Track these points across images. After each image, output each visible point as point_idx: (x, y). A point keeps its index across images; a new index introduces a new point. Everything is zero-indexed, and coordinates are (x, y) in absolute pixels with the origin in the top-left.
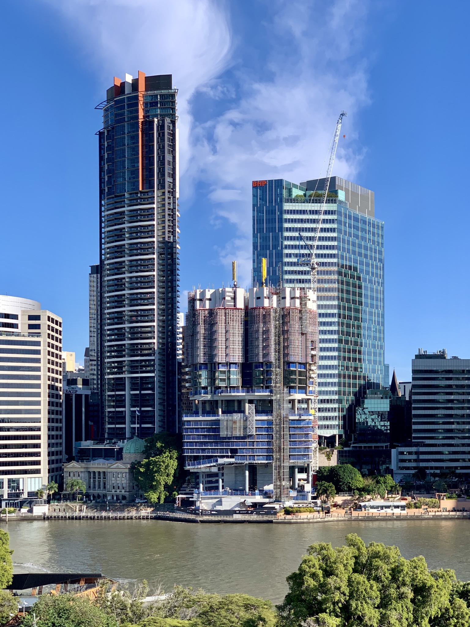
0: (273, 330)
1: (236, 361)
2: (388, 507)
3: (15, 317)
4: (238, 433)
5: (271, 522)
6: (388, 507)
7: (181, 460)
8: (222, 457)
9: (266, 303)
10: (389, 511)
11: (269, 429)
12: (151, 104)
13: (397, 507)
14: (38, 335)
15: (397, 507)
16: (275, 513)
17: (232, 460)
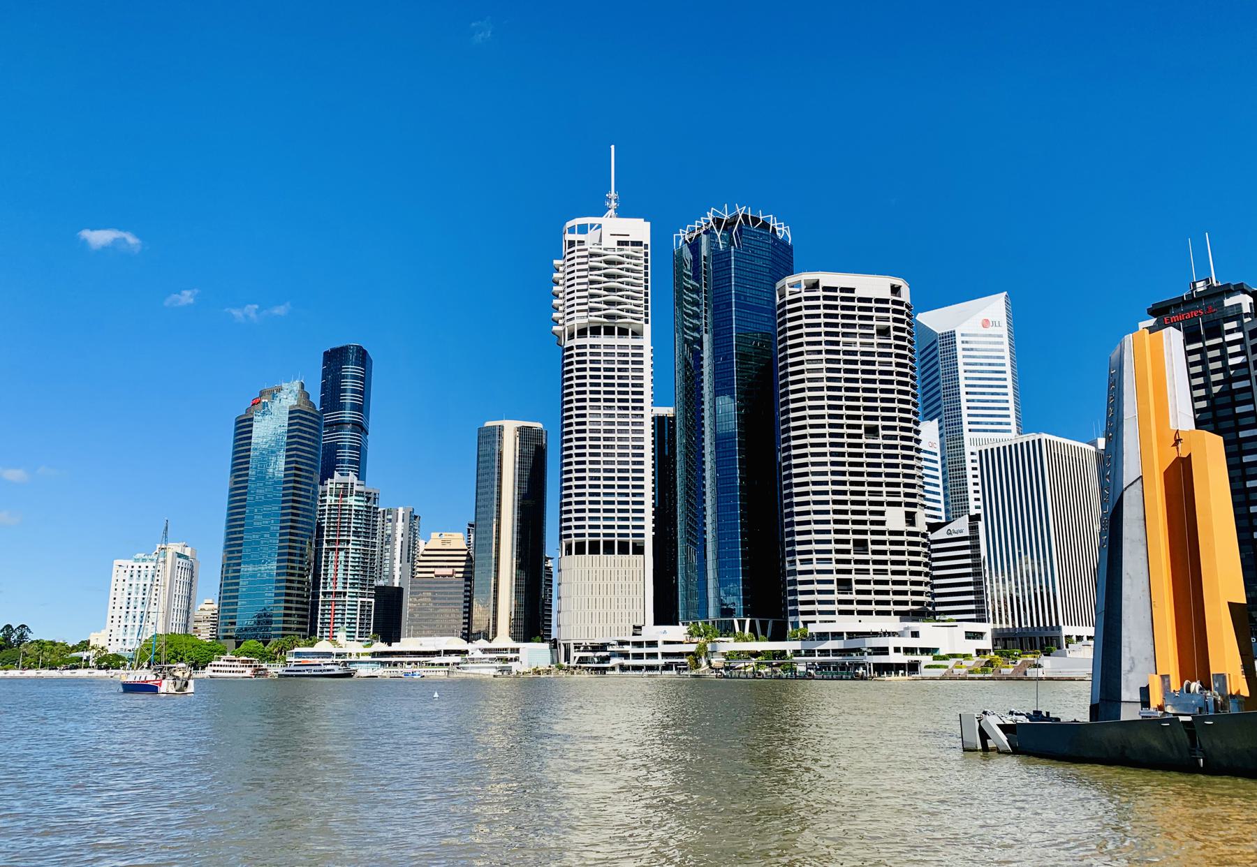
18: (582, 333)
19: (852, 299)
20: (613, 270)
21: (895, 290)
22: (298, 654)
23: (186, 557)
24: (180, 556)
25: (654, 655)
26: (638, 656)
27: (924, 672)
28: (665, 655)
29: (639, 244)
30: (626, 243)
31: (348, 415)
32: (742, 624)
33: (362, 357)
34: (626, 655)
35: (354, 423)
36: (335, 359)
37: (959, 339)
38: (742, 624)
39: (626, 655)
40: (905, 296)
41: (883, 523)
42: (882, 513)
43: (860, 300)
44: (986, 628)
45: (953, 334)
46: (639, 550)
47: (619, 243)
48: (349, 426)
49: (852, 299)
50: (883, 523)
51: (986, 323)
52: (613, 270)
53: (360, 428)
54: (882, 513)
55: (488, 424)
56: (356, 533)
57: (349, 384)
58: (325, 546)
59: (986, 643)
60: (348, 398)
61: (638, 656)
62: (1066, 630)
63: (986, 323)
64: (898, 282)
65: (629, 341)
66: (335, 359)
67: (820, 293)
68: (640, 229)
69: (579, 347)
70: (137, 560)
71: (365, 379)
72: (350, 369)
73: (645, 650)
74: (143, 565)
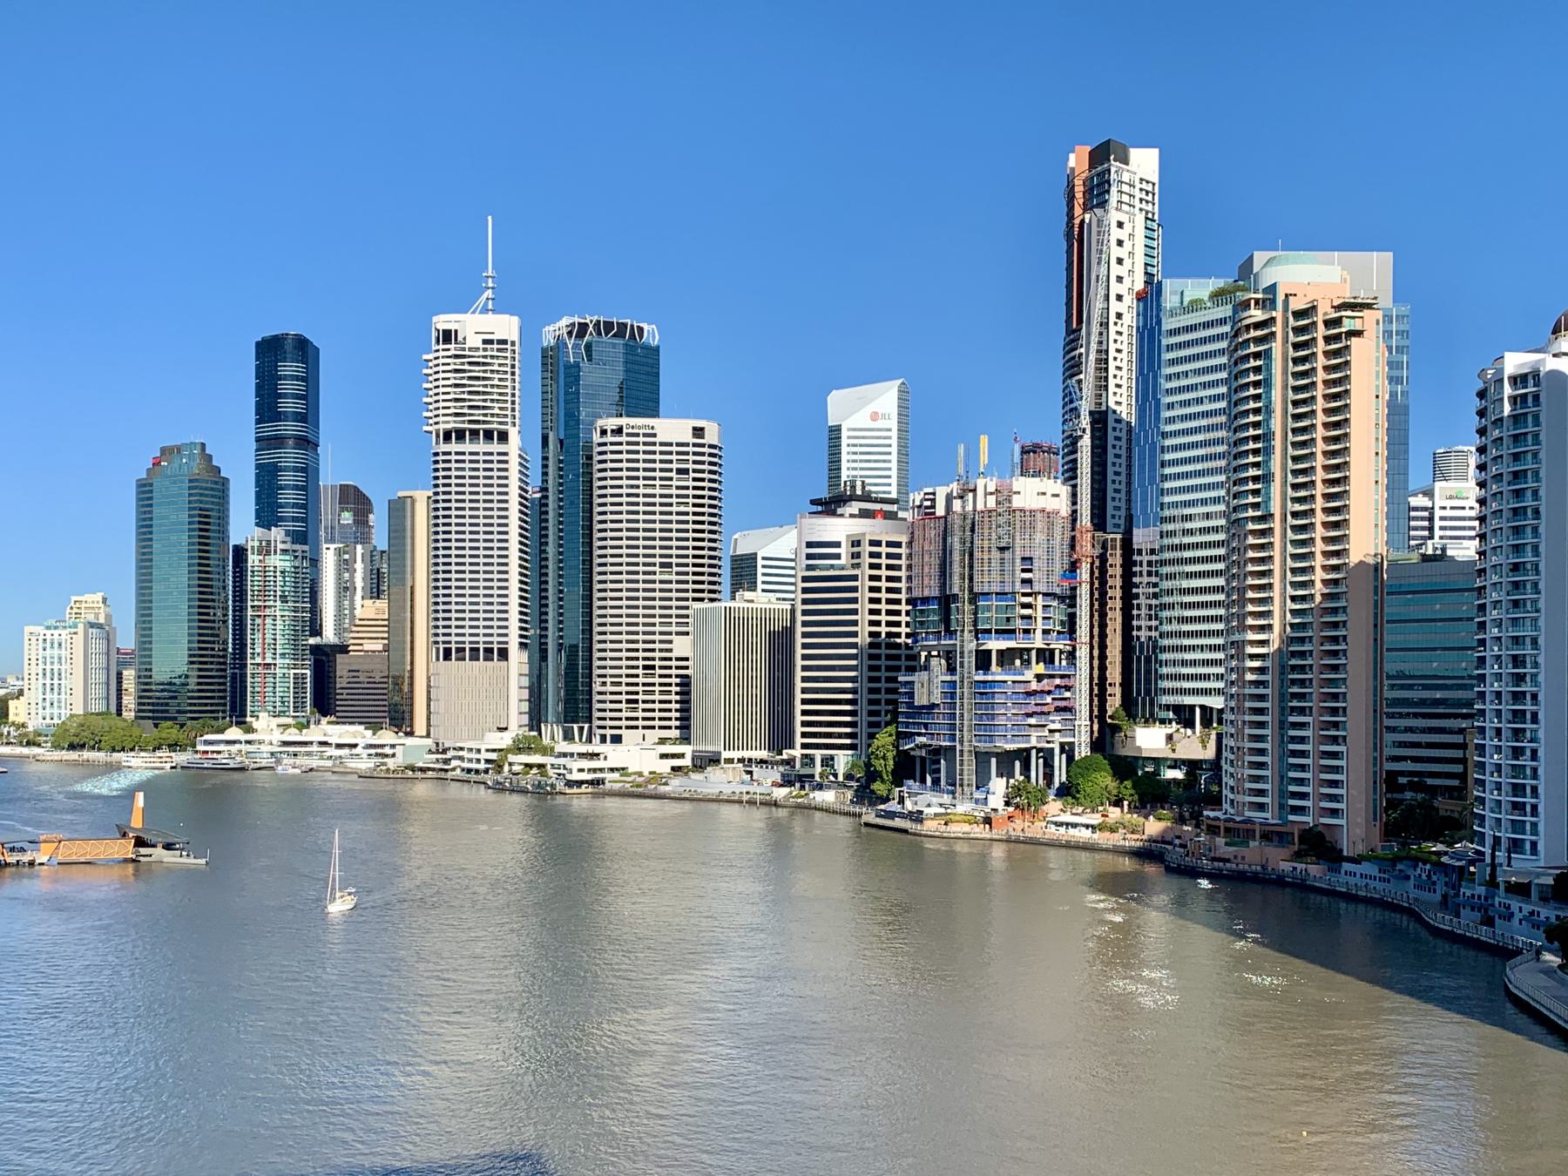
0: (957, 546)
1: (935, 593)
2: (1075, 825)
3: (838, 545)
4: (925, 703)
5: (905, 831)
6: (1075, 825)
7: (899, 734)
8: (920, 734)
9: (957, 505)
10: (1071, 831)
11: (953, 695)
12: (1088, 192)
13: (1087, 826)
14: (857, 566)
15: (1087, 826)
16: (921, 821)
17: (923, 739)
18: (447, 436)
19: (654, 444)
20: (477, 371)
21: (698, 432)
22: (207, 743)
23: (100, 626)
24: (92, 625)
25: (478, 761)
26: (470, 760)
27: (608, 785)
28: (487, 761)
29: (504, 342)
30: (491, 342)
31: (289, 428)
32: (581, 729)
33: (304, 349)
34: (461, 758)
35: (297, 438)
36: (270, 350)
37: (844, 434)
38: (581, 729)
39: (461, 758)
40: (711, 437)
41: (670, 650)
42: (671, 642)
43: (662, 444)
44: (687, 750)
45: (838, 429)
46: (504, 654)
47: (485, 342)
48: (291, 442)
49: (654, 444)
50: (670, 650)
51: (875, 416)
52: (477, 371)
53: (308, 443)
54: (671, 642)
55: (401, 494)
56: (284, 599)
57: (287, 387)
58: (250, 612)
59: (687, 762)
60: (288, 406)
61: (470, 760)
62: (725, 755)
63: (874, 416)
64: (699, 424)
65: (495, 447)
66: (270, 350)
67: (624, 439)
68: (507, 326)
69: (445, 453)
70: (48, 628)
71: (310, 380)
72: (289, 368)
73: (474, 756)
74: (56, 632)
